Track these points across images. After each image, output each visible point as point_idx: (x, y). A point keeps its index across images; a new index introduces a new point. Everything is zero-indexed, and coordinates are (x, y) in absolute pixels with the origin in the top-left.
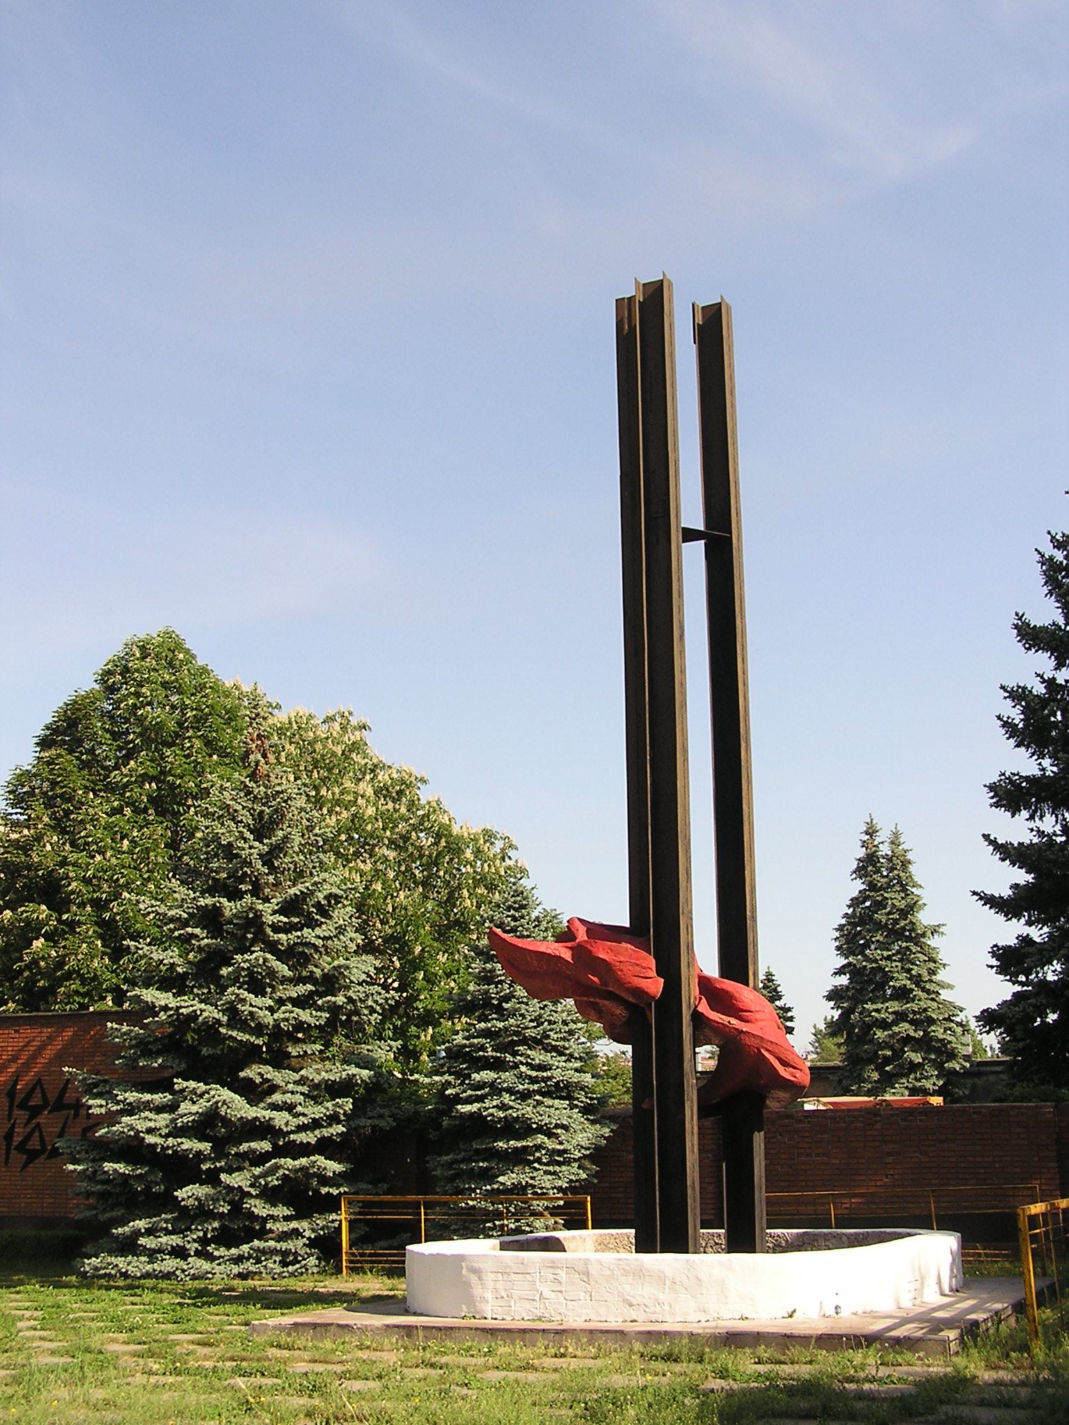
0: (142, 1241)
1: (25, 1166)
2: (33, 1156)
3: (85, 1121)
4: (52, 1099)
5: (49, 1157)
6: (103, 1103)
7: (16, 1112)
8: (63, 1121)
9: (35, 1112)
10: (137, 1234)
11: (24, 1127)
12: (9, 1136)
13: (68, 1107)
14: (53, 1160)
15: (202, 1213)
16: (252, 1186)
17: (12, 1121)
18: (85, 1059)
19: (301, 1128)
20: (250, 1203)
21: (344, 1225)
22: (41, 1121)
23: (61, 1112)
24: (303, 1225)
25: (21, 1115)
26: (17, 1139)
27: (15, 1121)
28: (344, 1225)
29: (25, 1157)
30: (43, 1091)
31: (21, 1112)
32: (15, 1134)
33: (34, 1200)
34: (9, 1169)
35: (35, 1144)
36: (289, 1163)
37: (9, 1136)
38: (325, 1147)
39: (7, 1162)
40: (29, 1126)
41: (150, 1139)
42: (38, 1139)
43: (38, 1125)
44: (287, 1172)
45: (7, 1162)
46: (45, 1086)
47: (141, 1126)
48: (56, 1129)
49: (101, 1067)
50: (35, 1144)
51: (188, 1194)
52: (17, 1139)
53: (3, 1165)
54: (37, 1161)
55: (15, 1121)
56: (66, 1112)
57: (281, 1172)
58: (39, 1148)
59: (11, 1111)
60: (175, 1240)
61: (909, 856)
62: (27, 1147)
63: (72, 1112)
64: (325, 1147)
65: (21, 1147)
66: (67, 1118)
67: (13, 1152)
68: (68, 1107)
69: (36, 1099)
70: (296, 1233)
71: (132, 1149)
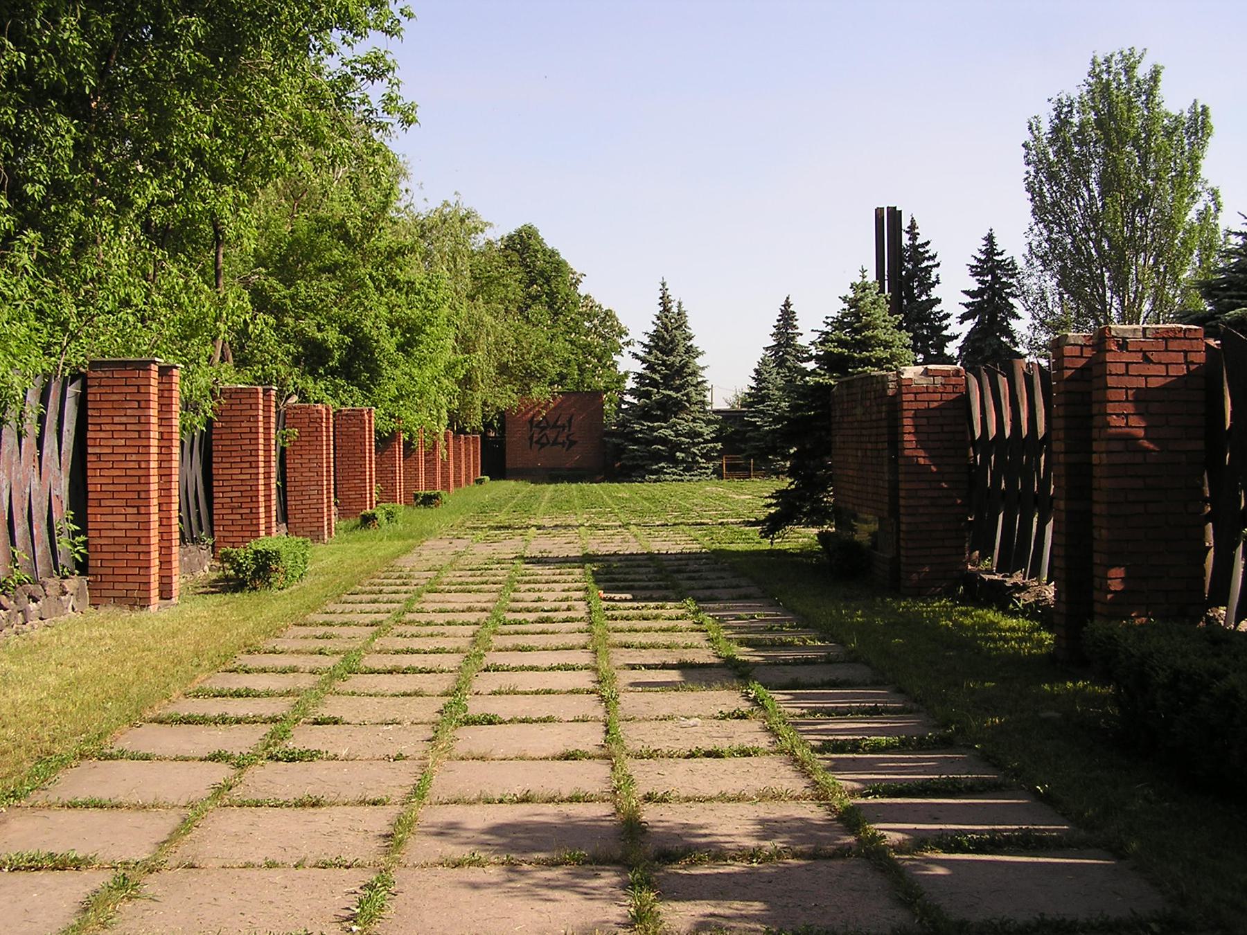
0: (665, 470)
1: (541, 448)
2: (543, 445)
4: (551, 423)
5: (552, 445)
9: (543, 429)
10: (664, 468)
12: (531, 438)
15: (683, 461)
19: (707, 434)
20: (698, 458)
26: (535, 440)
30: (547, 421)
35: (544, 440)
36: (709, 445)
37: (531, 438)
38: (713, 440)
41: (671, 438)
50: (544, 440)
52: (535, 440)
56: (558, 429)
59: (531, 428)
60: (674, 469)
61: (687, 314)
64: (713, 440)
65: (537, 442)
67: (534, 445)
68: (559, 427)
70: (708, 468)
71: (664, 441)
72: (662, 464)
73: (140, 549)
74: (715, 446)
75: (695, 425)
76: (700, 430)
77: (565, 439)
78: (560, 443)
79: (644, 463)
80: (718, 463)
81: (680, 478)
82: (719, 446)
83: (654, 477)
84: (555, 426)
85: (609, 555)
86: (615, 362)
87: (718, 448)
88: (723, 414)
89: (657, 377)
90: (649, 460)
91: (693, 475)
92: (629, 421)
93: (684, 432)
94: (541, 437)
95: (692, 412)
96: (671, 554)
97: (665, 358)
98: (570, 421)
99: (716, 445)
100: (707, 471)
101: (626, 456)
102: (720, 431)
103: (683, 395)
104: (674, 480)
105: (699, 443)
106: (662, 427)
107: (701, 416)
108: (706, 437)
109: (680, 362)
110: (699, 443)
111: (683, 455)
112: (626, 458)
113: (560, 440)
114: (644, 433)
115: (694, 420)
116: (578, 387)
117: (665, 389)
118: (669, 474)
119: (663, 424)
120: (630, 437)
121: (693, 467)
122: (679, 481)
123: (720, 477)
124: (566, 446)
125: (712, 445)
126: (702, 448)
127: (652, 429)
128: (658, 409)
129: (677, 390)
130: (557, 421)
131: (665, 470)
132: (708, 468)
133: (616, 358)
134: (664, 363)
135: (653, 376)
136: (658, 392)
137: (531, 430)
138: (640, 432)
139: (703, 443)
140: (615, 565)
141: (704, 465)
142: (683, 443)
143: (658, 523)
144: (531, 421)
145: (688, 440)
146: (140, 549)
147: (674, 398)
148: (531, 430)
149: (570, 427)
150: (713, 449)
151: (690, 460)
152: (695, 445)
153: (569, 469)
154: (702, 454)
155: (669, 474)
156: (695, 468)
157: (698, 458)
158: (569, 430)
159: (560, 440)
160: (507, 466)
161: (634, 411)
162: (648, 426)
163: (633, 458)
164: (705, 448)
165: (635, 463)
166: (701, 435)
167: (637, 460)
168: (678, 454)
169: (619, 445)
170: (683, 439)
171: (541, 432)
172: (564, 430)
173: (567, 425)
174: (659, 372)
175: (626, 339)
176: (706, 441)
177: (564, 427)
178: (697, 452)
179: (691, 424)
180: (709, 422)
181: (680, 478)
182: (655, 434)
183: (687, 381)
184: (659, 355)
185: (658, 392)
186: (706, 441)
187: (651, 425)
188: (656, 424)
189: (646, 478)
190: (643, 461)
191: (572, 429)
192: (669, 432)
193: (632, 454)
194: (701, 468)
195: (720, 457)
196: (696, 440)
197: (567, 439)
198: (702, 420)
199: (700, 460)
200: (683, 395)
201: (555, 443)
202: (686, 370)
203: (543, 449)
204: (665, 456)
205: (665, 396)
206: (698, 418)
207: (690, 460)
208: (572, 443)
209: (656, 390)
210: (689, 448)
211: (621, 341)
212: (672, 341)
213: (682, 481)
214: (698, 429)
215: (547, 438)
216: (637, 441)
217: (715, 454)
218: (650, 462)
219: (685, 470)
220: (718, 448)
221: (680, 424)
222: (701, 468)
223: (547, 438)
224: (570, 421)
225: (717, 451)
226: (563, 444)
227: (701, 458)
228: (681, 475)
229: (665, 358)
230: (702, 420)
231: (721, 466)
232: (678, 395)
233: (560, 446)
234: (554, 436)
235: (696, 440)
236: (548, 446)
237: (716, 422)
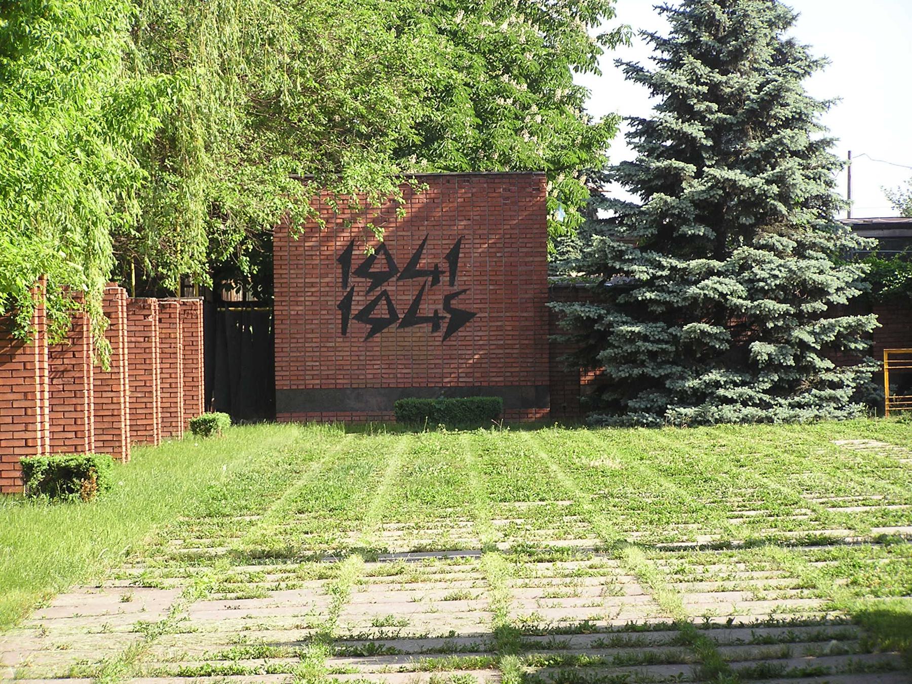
0: (721, 392)
1: (372, 334)
2: (379, 326)
3: (448, 288)
4: (401, 267)
5: (403, 325)
6: (644, 269)
7: (352, 280)
8: (420, 288)
9: (379, 279)
11: (366, 296)
12: (345, 305)
13: (422, 273)
14: (407, 329)
15: (771, 365)
16: (816, 342)
17: (348, 289)
18: (444, 223)
20: (812, 357)
21: (886, 374)
22: (389, 288)
23: (414, 279)
24: (848, 377)
25: (360, 284)
26: (355, 309)
27: (352, 288)
28: (886, 374)
29: (369, 326)
30: (389, 257)
31: (358, 279)
32: (353, 303)
33: (383, 371)
34: (348, 340)
36: (845, 320)
37: (345, 305)
38: (855, 306)
39: (344, 332)
40: (372, 294)
42: (386, 307)
43: (385, 293)
44: (842, 329)
45: (344, 332)
46: (390, 252)
47: (724, 289)
48: (410, 297)
49: (466, 232)
50: (381, 312)
51: (762, 349)
52: (355, 309)
53: (340, 335)
54: (386, 330)
55: (352, 288)
57: (837, 328)
58: (388, 316)
60: (745, 390)
62: (370, 316)
63: (430, 279)
64: (855, 306)
65: (362, 316)
66: (424, 285)
67: (353, 324)
68: (422, 273)
69: (379, 266)
72: (714, 376)
73: (193, 348)
74: (860, 325)
75: (803, 263)
76: (816, 277)
77: (440, 306)
78: (426, 320)
79: (662, 372)
80: (868, 369)
81: (763, 413)
82: (871, 322)
83: (690, 411)
84: (410, 271)
85: (568, 631)
86: (576, 90)
87: (869, 328)
88: (886, 233)
89: (695, 130)
90: (675, 363)
91: (800, 406)
92: (619, 255)
93: (773, 283)
94: (375, 302)
95: (795, 227)
96: (742, 626)
97: (718, 77)
98: (453, 257)
99: (863, 319)
100: (839, 393)
101: (609, 351)
102: (874, 279)
103: (768, 182)
104: (744, 420)
105: (815, 316)
106: (710, 273)
107: (819, 238)
108: (834, 298)
109: (760, 88)
110: (815, 316)
111: (771, 348)
112: (613, 360)
113: (427, 309)
114: (661, 289)
115: (800, 251)
116: (474, 161)
117: (718, 165)
118: (731, 401)
119: (716, 264)
120: (621, 299)
121: (798, 382)
122: (760, 421)
123: (876, 407)
124: (444, 326)
125: (851, 320)
126: (825, 330)
127: (683, 278)
128: (700, 220)
129: (753, 166)
130: (417, 257)
131: (721, 392)
132: (839, 385)
133: (580, 79)
134: (714, 93)
135: (687, 128)
136: (699, 175)
137: (345, 284)
138: (650, 284)
139: (825, 314)
140: (585, 659)
141: (830, 376)
142: (762, 318)
143: (703, 540)
144: (345, 258)
145: (784, 307)
146: (193, 348)
147: (744, 190)
148: (345, 284)
149: (453, 275)
150: (853, 332)
151: (791, 362)
152: (802, 319)
153: (452, 392)
154: (825, 345)
155: (731, 401)
156: (805, 385)
157: (812, 357)
158: (452, 284)
159: (427, 309)
160: (281, 383)
161: (632, 227)
162: (673, 269)
163: (631, 359)
164: (831, 328)
165: (636, 371)
166: (819, 292)
167: (642, 364)
168: (756, 346)
169: (591, 321)
170: (770, 304)
171: (372, 289)
172: (436, 281)
173: (444, 266)
174: (700, 117)
175: (607, 26)
176: (834, 310)
177: (436, 273)
178: (810, 339)
179: (792, 263)
180: (842, 257)
181: (763, 413)
182: (693, 290)
183: (780, 142)
184: (703, 70)
185: (699, 175)
186: (834, 310)
187: (681, 265)
188: (693, 263)
189: (669, 413)
190: (660, 365)
191: (460, 278)
192: (729, 285)
193: (628, 348)
194: (821, 385)
195: (873, 353)
196: (807, 307)
197: (447, 307)
198: (824, 250)
199: (819, 363)
200: (768, 182)
201: (412, 318)
202: (777, 110)
203: (378, 337)
204: (720, 353)
205: (718, 183)
206: (813, 246)
207: (791, 362)
208: (460, 319)
209: (692, 168)
210: (788, 329)
211: (593, 32)
212: (736, 31)
213: (770, 420)
214: (812, 276)
215: (389, 303)
216: (640, 311)
217: (861, 346)
218: (677, 369)
219: (776, 390)
220: (869, 328)
221: (760, 263)
222: (821, 385)
223: (389, 303)
224: (453, 257)
225: (866, 336)
226: (435, 321)
227: (822, 355)
228: (766, 406)
229: (718, 77)
230: (824, 250)
231: (877, 377)
232: (756, 180)
233: (427, 328)
234: (410, 298)
235: (807, 307)
236: (393, 327)
237: (861, 255)
